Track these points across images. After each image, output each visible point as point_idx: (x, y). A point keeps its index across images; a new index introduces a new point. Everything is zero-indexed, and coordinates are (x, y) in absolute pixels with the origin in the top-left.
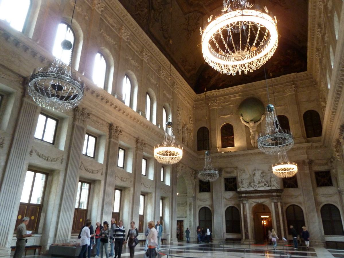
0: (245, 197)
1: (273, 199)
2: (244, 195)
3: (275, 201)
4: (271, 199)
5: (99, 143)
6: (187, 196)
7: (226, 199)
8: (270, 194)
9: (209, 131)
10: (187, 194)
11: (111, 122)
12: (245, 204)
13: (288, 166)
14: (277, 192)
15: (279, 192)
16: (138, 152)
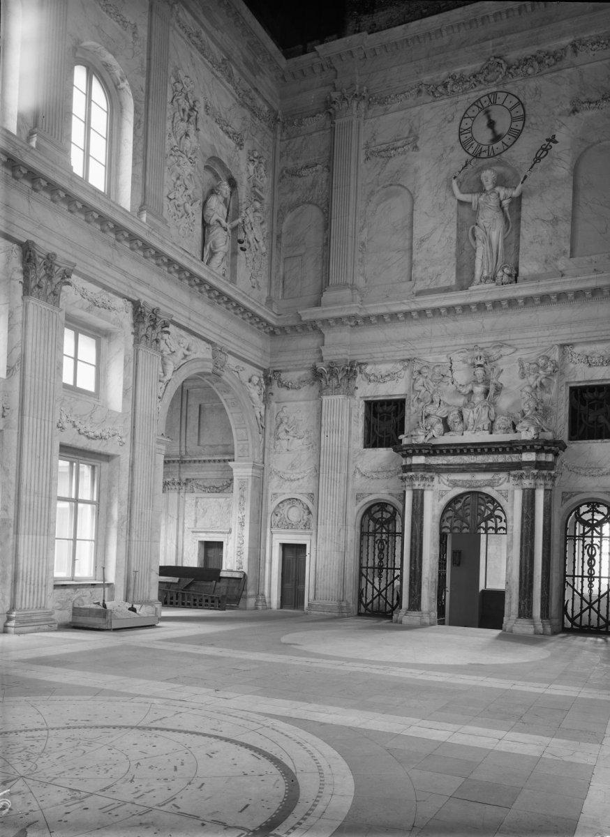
0: (427, 468)
1: (521, 477)
4: (515, 476)
8: (514, 458)
14: (538, 452)
15: (547, 452)
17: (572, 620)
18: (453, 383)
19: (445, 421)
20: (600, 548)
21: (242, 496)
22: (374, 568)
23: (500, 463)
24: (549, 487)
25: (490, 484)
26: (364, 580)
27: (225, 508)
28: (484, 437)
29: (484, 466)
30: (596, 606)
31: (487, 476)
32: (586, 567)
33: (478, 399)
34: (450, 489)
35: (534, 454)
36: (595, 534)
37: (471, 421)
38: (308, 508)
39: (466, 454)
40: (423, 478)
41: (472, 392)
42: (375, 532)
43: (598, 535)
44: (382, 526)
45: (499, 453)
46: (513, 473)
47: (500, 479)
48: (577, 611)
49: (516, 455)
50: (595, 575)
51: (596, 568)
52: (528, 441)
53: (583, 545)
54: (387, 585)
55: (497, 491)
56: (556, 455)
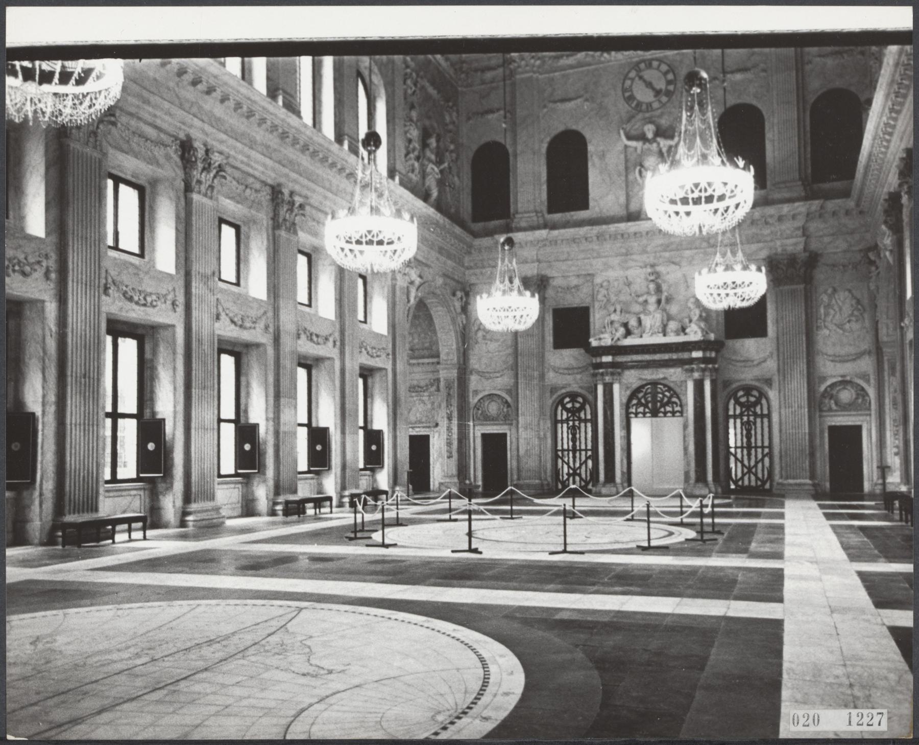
0: (613, 365)
1: (692, 370)
2: (607, 359)
3: (696, 375)
5: (153, 210)
6: (438, 363)
7: (556, 370)
8: (685, 355)
9: (511, 158)
10: (438, 356)
11: (188, 136)
12: (611, 384)
13: (738, 275)
14: (704, 350)
15: (711, 350)
16: (283, 233)
17: (735, 482)
19: (625, 325)
21: (449, 394)
22: (568, 450)
26: (560, 461)
27: (429, 406)
28: (659, 339)
30: (754, 470)
32: (745, 440)
33: (652, 307)
37: (648, 326)
38: (507, 402)
40: (612, 374)
41: (646, 301)
42: (568, 420)
44: (573, 415)
46: (687, 367)
48: (739, 475)
51: (753, 440)
54: (581, 464)
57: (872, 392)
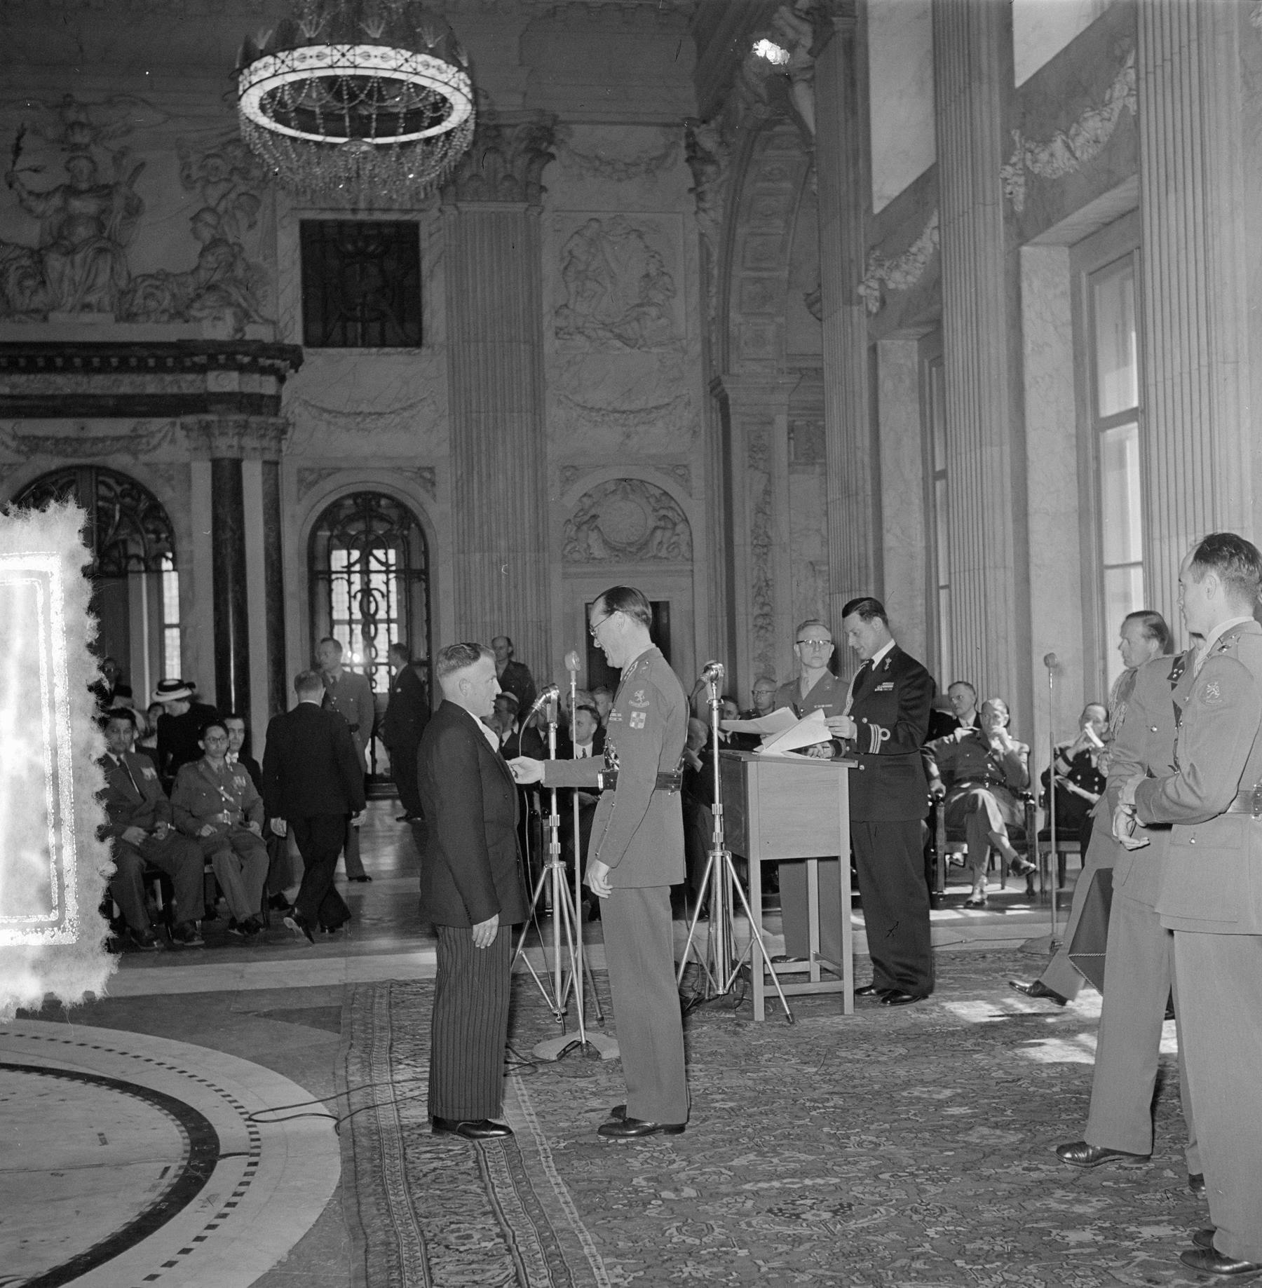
15: (264, 371)
18: (11, 186)
20: (386, 596)
23: (148, 396)
24: (270, 456)
25: (131, 443)
29: (111, 402)
31: (123, 426)
34: (22, 459)
35: (235, 375)
36: (374, 565)
39: (63, 370)
43: (383, 568)
45: (149, 370)
47: (152, 434)
49: (190, 377)
50: (379, 660)
52: (221, 344)
53: (349, 592)
55: (147, 465)
56: (282, 379)
57: (697, 508)
